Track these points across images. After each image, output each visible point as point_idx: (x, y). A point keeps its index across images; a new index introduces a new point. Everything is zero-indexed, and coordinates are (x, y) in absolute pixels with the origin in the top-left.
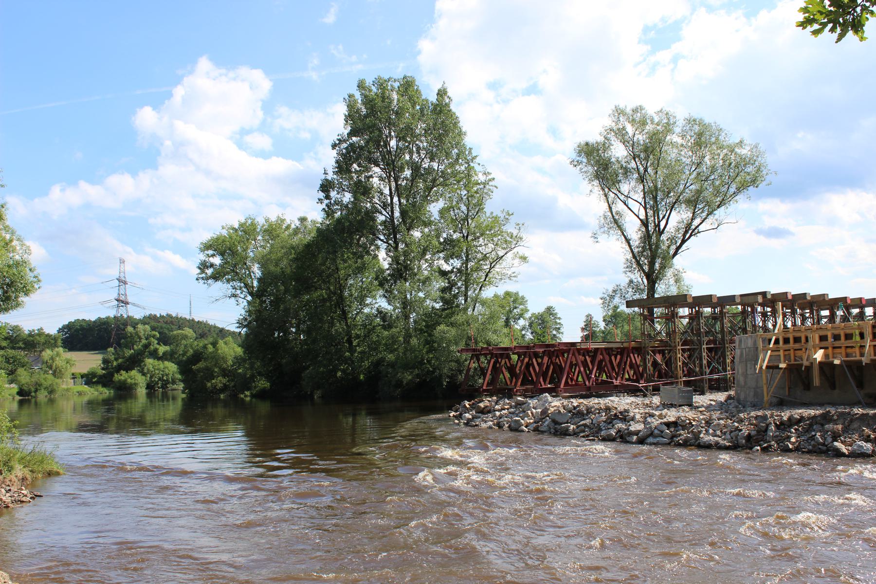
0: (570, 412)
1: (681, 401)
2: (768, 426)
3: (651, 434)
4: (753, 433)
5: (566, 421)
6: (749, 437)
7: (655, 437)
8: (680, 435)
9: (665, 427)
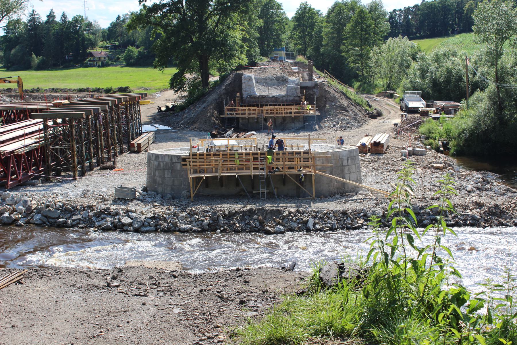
0: (58, 209)
1: (132, 197)
2: (218, 217)
3: (143, 225)
4: (211, 222)
5: (57, 216)
6: (209, 225)
7: (146, 226)
8: (161, 225)
9: (150, 220)
